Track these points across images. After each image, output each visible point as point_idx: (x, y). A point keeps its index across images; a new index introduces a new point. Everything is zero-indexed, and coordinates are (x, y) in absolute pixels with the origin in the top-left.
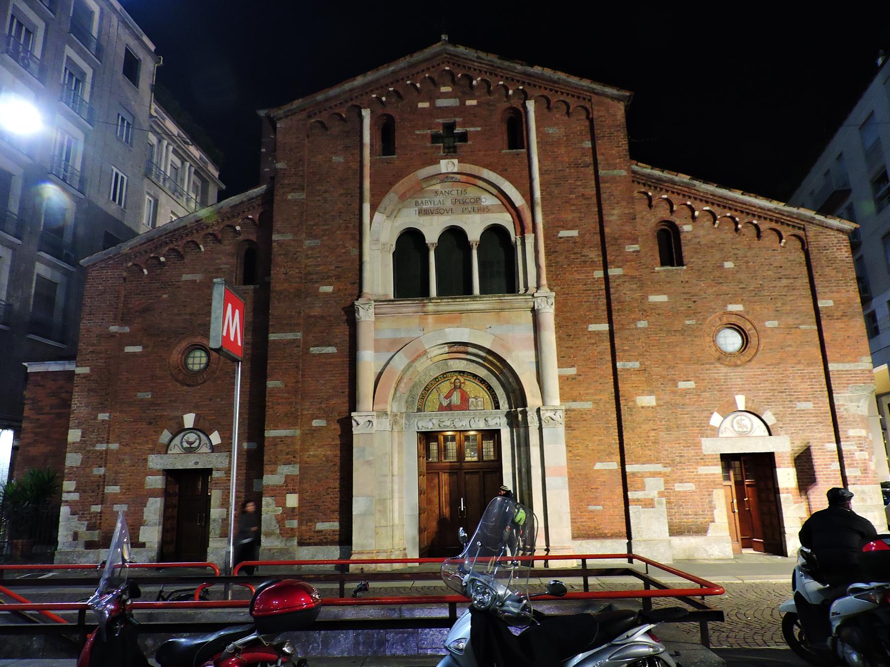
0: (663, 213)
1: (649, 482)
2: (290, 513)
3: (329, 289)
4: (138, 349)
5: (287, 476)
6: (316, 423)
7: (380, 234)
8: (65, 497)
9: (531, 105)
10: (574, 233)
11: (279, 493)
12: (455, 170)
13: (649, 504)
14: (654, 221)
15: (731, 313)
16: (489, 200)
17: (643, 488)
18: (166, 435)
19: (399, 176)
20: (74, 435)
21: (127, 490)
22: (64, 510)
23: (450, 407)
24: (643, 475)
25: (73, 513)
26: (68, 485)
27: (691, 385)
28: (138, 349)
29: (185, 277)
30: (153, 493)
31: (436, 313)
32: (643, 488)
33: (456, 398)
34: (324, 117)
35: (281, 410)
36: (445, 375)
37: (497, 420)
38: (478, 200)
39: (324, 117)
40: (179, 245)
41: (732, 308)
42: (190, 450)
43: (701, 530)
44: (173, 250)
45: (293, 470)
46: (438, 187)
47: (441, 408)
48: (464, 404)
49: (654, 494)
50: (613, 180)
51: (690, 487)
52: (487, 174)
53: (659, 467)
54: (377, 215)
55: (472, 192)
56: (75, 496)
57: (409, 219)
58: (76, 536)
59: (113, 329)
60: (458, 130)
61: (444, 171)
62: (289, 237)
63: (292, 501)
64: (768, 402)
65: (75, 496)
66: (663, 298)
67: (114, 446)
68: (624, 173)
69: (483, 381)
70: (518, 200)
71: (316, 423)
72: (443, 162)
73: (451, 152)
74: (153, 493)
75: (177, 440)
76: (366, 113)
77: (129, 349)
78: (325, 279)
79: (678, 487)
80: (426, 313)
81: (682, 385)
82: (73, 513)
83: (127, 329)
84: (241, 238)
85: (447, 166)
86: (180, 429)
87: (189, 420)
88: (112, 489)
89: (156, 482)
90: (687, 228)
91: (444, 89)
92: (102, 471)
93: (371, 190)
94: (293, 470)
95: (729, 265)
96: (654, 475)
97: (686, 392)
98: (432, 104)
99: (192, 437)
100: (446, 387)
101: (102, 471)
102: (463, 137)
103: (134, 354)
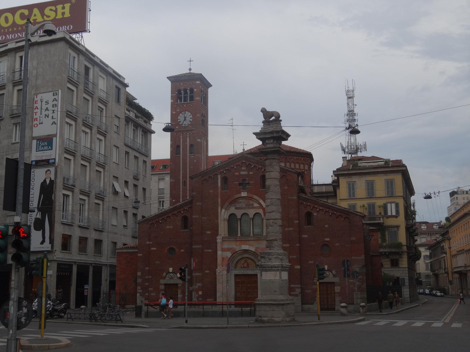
2: (199, 296)
3: (209, 232)
4: (155, 249)
5: (199, 286)
6: (206, 272)
8: (138, 291)
11: (197, 291)
12: (246, 195)
15: (326, 241)
16: (256, 205)
17: (295, 291)
18: (165, 274)
20: (139, 274)
22: (138, 295)
23: (244, 267)
25: (141, 296)
26: (139, 288)
27: (312, 262)
28: (155, 249)
29: (168, 227)
31: (239, 240)
32: (295, 291)
33: (245, 265)
36: (243, 258)
37: (256, 271)
38: (253, 205)
42: (171, 278)
44: (163, 219)
46: (241, 200)
47: (241, 268)
48: (248, 266)
49: (298, 293)
51: (309, 291)
52: (255, 197)
53: (300, 286)
54: (223, 210)
55: (251, 202)
56: (141, 291)
57: (232, 210)
58: (142, 302)
59: (148, 243)
60: (247, 182)
61: (243, 196)
62: (197, 216)
63: (200, 293)
65: (141, 291)
66: (306, 236)
67: (150, 277)
68: (295, 198)
69: (253, 260)
71: (206, 272)
72: (242, 193)
73: (244, 189)
75: (168, 276)
76: (219, 176)
77: (153, 249)
80: (237, 241)
81: (310, 262)
82: (141, 296)
83: (151, 243)
84: (182, 215)
85: (244, 194)
86: (169, 273)
87: (171, 270)
88: (151, 289)
89: (162, 287)
90: (315, 214)
91: (243, 168)
92: (148, 284)
93: (221, 201)
95: (326, 226)
96: (298, 288)
98: (240, 173)
99: (172, 275)
100: (243, 261)
101: (148, 284)
102: (249, 183)
103: (154, 250)
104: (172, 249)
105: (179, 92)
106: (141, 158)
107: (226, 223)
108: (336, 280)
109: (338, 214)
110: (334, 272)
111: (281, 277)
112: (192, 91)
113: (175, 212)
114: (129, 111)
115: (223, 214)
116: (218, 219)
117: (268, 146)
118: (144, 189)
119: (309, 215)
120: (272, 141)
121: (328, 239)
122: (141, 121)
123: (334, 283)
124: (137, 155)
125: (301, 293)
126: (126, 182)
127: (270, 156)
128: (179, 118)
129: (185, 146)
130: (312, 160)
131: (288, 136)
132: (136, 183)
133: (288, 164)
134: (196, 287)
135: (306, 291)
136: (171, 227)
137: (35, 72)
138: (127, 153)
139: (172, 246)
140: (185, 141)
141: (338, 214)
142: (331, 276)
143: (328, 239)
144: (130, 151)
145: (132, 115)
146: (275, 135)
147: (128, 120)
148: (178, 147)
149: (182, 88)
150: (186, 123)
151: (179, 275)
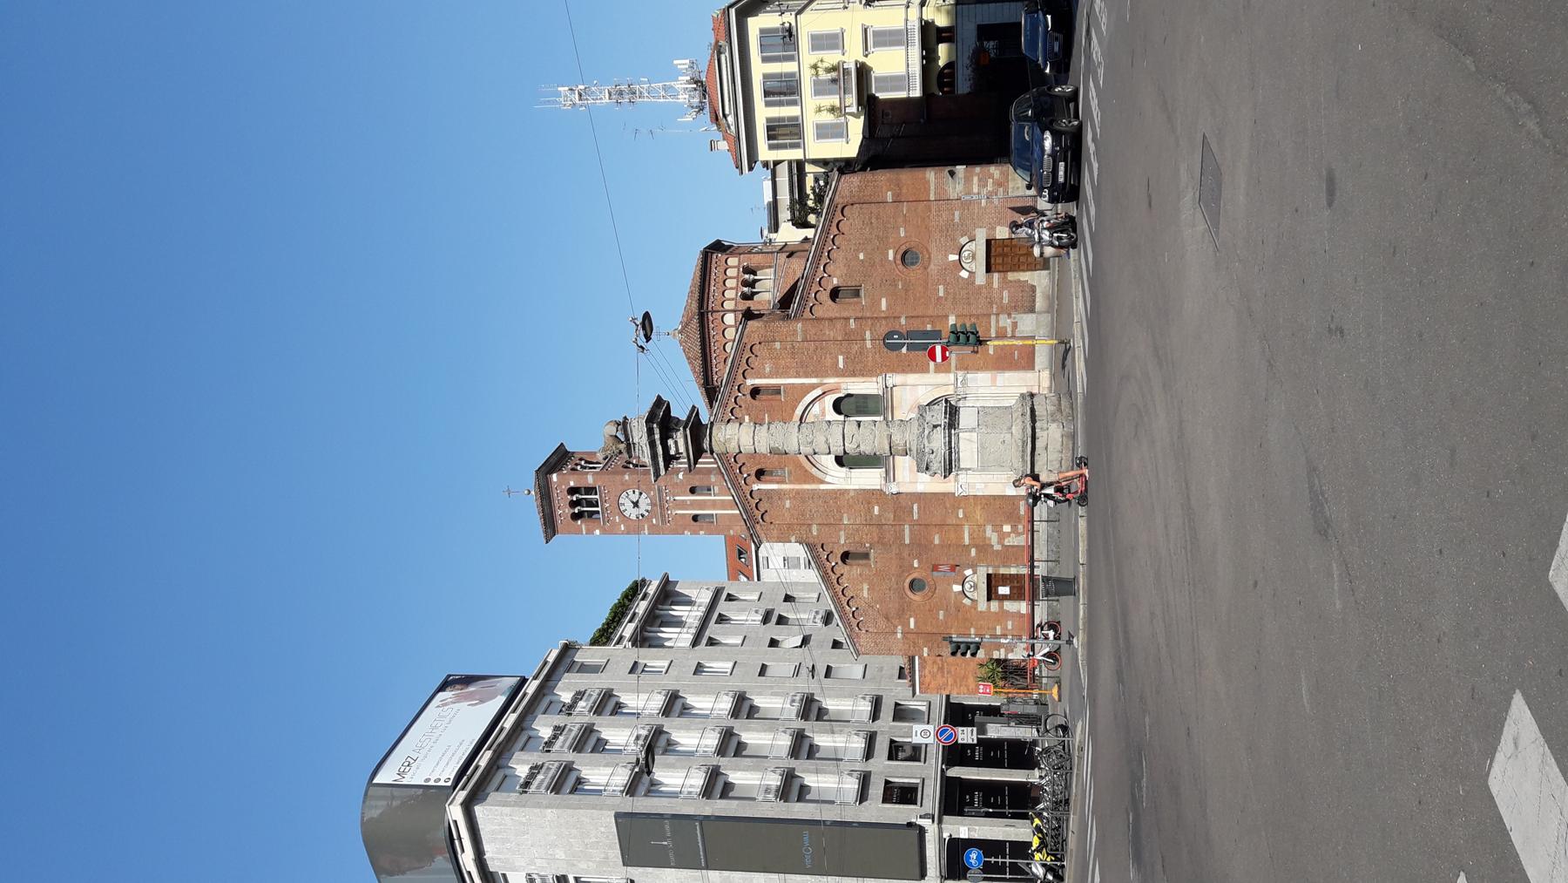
0: (824, 296)
1: (1001, 324)
2: (1014, 527)
7: (839, 479)
9: (750, 382)
10: (841, 358)
13: (1015, 325)
14: (830, 302)
16: (816, 409)
18: (966, 601)
19: (801, 467)
21: (999, 622)
22: (1010, 656)
24: (997, 327)
30: (1001, 607)
34: (758, 514)
35: (952, 536)
39: (758, 514)
40: (844, 600)
41: (891, 257)
42: (975, 587)
43: (1033, 289)
45: (989, 528)
50: (805, 332)
51: (1005, 294)
53: (993, 318)
54: (828, 479)
55: (810, 419)
63: (1007, 528)
64: (954, 240)
66: (884, 301)
70: (818, 392)
74: (1001, 607)
76: (755, 487)
77: (912, 626)
78: (870, 510)
79: (1006, 301)
87: (957, 588)
89: (994, 605)
90: (835, 281)
94: (989, 528)
95: (861, 256)
97: (946, 290)
99: (967, 586)
104: (912, 583)
105: (575, 517)
106: (723, 607)
107: (856, 472)
108: (981, 236)
109: (834, 230)
110: (964, 240)
111: (973, 430)
112: (572, 491)
113: (834, 577)
114: (621, 637)
115: (839, 479)
116: (847, 491)
117: (682, 449)
118: (788, 598)
119: (835, 294)
120: (670, 442)
121: (891, 253)
122: (641, 607)
123: (988, 242)
124: (715, 616)
125: (1009, 315)
126: (774, 643)
127: (706, 445)
128: (633, 517)
129: (693, 505)
130: (718, 247)
131: (659, 402)
132: (774, 619)
133: (728, 305)
134: (994, 538)
135: (1006, 301)
136: (866, 587)
137: (538, 862)
138: (712, 642)
139: (907, 585)
140: (683, 505)
141: (834, 230)
142: (971, 246)
143: (891, 253)
144: (707, 634)
145: (628, 629)
146: (657, 436)
147: (642, 639)
148: (695, 518)
149: (569, 511)
150: (645, 504)
151: (968, 572)
